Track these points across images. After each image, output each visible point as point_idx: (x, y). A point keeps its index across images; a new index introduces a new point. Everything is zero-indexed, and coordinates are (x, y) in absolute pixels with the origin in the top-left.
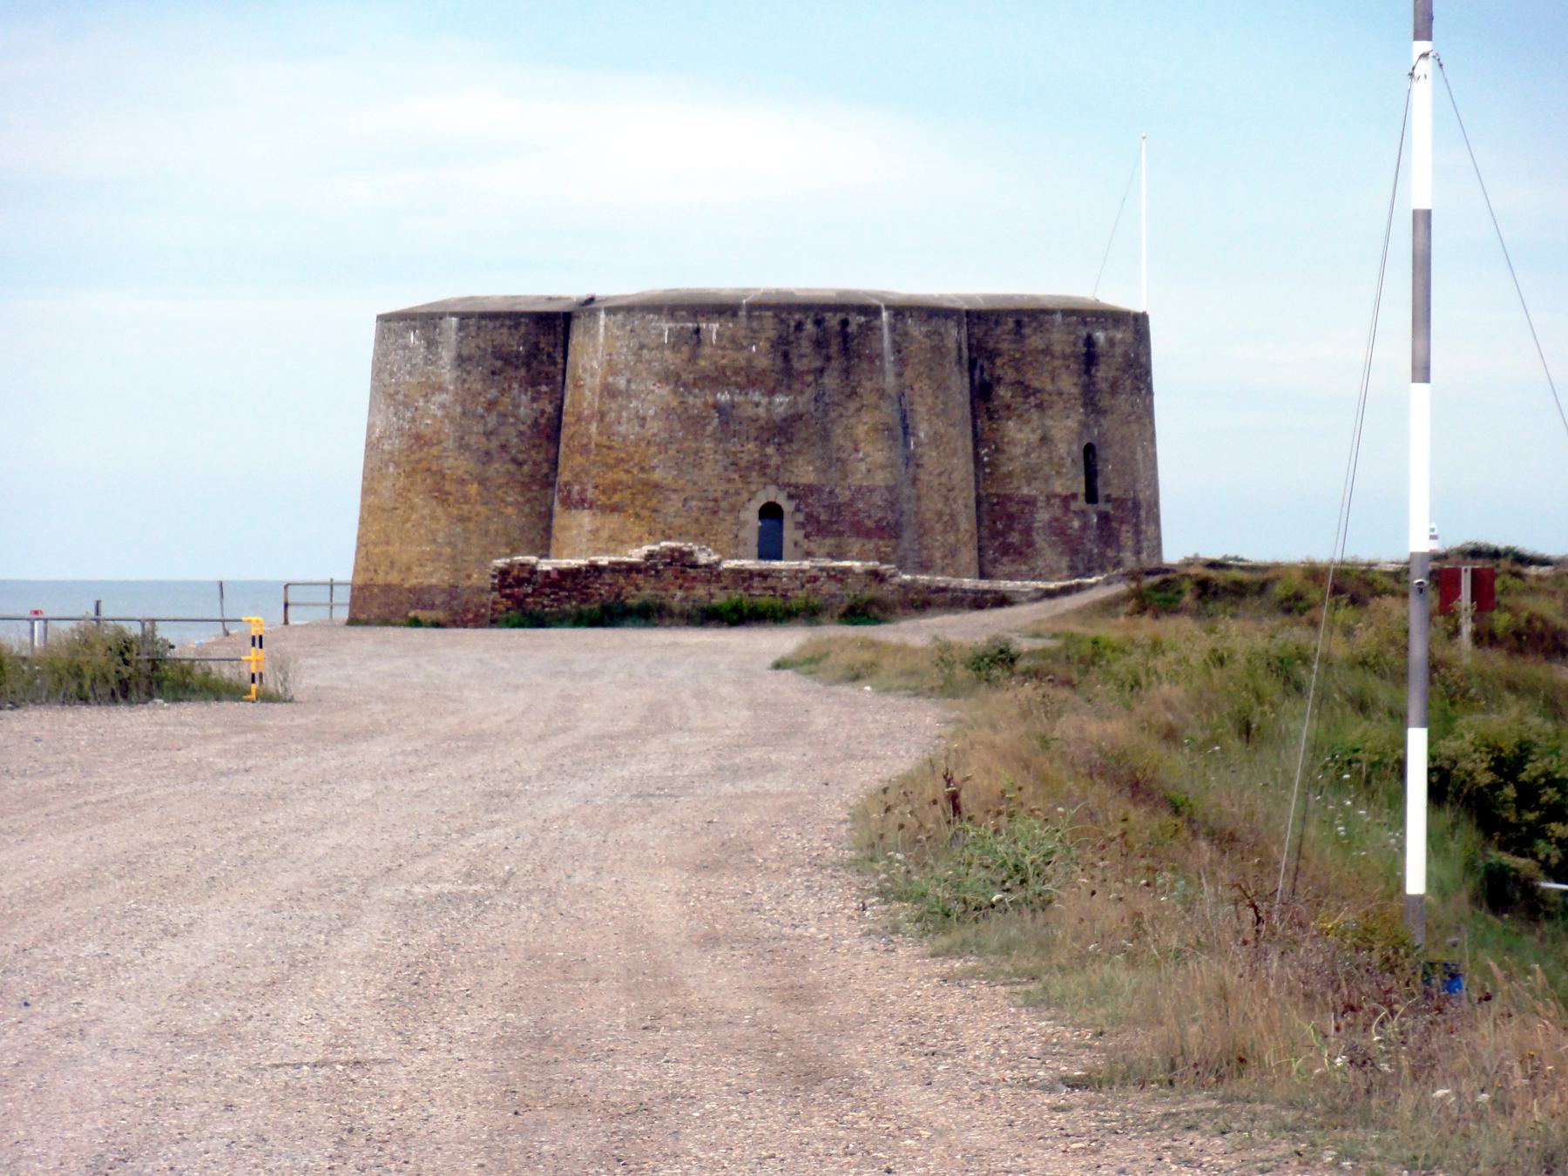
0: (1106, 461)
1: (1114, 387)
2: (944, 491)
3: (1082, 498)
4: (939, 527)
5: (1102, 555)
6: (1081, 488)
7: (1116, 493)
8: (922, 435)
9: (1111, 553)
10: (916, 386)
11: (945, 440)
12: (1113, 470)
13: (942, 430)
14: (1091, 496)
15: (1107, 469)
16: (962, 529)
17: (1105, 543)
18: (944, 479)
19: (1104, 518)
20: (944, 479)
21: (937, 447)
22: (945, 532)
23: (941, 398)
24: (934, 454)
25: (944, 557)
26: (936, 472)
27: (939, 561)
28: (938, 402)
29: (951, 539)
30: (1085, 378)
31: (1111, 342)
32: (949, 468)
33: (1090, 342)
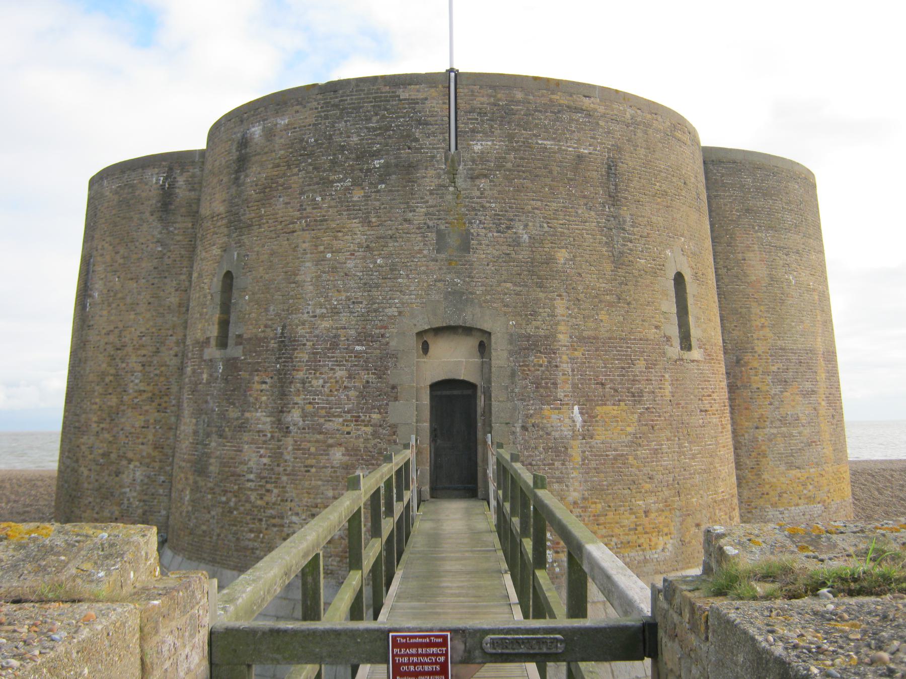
0: (244, 290)
1: (267, 191)
2: (110, 349)
3: (213, 342)
4: (99, 389)
5: (223, 415)
6: (214, 331)
7: (247, 331)
8: (96, 294)
9: (233, 413)
10: (100, 247)
11: (120, 295)
12: (250, 300)
13: (118, 287)
14: (223, 342)
15: (243, 301)
16: (131, 389)
17: (228, 399)
18: (111, 338)
19: (232, 365)
20: (111, 338)
21: (109, 305)
22: (106, 394)
23: (122, 251)
24: (105, 313)
25: (98, 423)
26: (104, 331)
27: (94, 425)
28: (118, 257)
29: (113, 401)
30: (233, 190)
31: (269, 134)
32: (120, 325)
33: (244, 143)
